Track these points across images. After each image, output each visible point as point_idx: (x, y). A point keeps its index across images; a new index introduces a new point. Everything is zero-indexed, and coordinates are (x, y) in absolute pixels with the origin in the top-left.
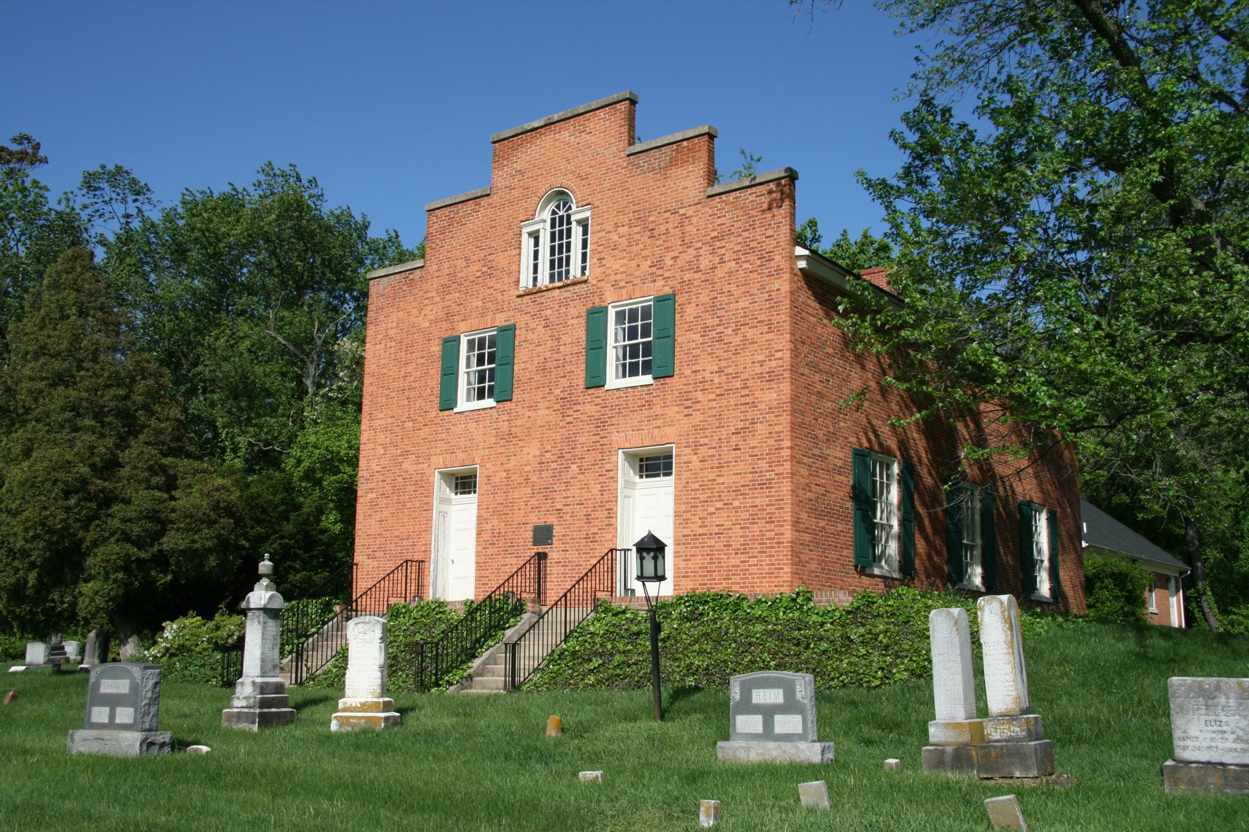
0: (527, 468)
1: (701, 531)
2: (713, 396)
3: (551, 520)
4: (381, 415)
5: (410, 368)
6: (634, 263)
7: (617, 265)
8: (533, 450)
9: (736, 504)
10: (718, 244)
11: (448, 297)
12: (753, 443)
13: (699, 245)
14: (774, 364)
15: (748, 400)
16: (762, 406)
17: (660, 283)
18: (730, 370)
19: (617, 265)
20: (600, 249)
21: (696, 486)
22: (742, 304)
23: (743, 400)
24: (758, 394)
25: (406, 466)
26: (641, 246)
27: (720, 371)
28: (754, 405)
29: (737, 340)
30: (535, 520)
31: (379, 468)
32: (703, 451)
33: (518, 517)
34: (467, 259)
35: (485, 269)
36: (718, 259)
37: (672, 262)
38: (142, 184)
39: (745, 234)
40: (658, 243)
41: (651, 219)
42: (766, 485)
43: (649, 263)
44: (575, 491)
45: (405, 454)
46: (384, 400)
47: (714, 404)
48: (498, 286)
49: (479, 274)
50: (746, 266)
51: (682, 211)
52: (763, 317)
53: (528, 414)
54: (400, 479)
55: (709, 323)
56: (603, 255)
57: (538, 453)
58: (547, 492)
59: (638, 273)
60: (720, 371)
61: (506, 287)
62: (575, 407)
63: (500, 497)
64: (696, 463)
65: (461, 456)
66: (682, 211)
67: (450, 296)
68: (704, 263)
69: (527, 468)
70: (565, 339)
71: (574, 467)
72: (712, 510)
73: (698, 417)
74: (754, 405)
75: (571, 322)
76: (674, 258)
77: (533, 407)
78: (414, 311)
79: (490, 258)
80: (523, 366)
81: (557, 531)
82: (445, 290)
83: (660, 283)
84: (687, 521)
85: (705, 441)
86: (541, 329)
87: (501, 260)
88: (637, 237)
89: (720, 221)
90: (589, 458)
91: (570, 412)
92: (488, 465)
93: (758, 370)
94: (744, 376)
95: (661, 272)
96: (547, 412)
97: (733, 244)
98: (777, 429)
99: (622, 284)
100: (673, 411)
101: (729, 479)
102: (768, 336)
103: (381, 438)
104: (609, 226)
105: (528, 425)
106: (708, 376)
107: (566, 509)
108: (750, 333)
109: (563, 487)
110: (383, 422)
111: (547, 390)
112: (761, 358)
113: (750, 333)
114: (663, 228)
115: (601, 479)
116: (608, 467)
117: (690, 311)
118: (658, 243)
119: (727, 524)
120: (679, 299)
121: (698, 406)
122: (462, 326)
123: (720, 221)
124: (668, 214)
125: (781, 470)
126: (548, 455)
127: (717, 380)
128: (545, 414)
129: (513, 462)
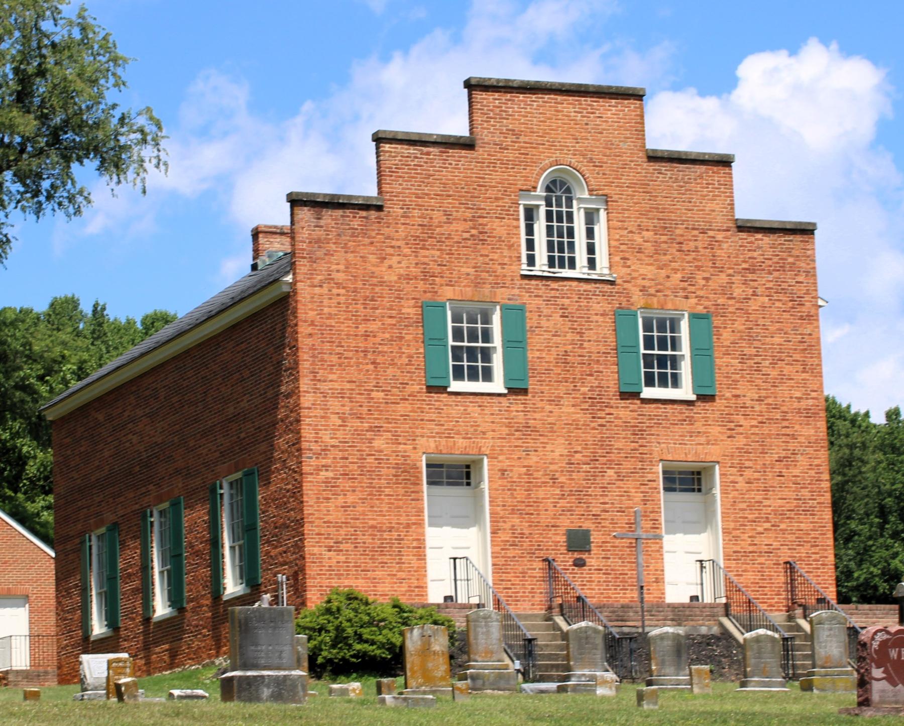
0: (552, 467)
1: (751, 549)
2: (754, 423)
3: (587, 525)
4: (331, 377)
5: (373, 326)
6: (663, 273)
7: (644, 270)
8: (558, 449)
9: (783, 526)
10: (750, 276)
11: (423, 252)
12: (796, 472)
13: (731, 271)
14: (811, 402)
15: (788, 431)
16: (802, 439)
17: (693, 301)
18: (770, 401)
19: (644, 270)
20: (623, 247)
21: (743, 506)
22: (777, 340)
23: (784, 431)
24: (797, 427)
25: (379, 443)
26: (669, 257)
27: (760, 400)
28: (794, 437)
29: (774, 373)
30: (567, 523)
31: (334, 442)
32: (748, 473)
33: (545, 519)
34: (447, 214)
35: (474, 232)
36: (750, 291)
37: (703, 282)
38: (878, 418)
39: (776, 274)
40: (689, 258)
41: (678, 232)
42: (810, 512)
43: (679, 276)
44: (613, 495)
45: (376, 430)
46: (334, 359)
47: (756, 430)
48: (496, 257)
49: (466, 235)
50: (778, 304)
51: (711, 233)
52: (797, 356)
53: (548, 408)
54: (370, 460)
55: (747, 351)
56: (627, 255)
57: (565, 452)
58: (580, 495)
59: (668, 284)
60: (760, 400)
61: (506, 260)
62: (608, 410)
63: (520, 494)
64: (741, 485)
65: (461, 442)
66: (711, 233)
67: (427, 253)
68: (738, 292)
69: (552, 467)
70: (588, 335)
71: (610, 472)
72: (760, 529)
73: (741, 441)
74: (794, 437)
75: (595, 318)
76: (707, 279)
77: (556, 401)
78: (372, 258)
79: (481, 221)
80: (537, 354)
81: (595, 538)
82: (419, 243)
83: (693, 301)
84: (736, 538)
85: (747, 464)
86: (557, 317)
87: (498, 228)
88: (664, 246)
89: (750, 254)
90: (628, 465)
91: (601, 414)
92: (501, 458)
93: (796, 405)
94: (784, 409)
95: (692, 289)
96: (572, 410)
97: (765, 280)
98: (816, 462)
99: (652, 291)
100: (715, 430)
101: (774, 502)
102: (804, 376)
103: (335, 405)
104: (632, 225)
105: (551, 420)
106: (749, 403)
107: (604, 515)
108: (787, 370)
109: (599, 492)
110: (336, 385)
111: (571, 387)
112: (798, 395)
113: (787, 370)
114: (692, 245)
115: (643, 488)
116: (650, 476)
117: (726, 336)
118: (689, 258)
119: (776, 544)
120: (717, 321)
121: (741, 430)
122: (448, 292)
123: (750, 254)
124: (696, 232)
125: (822, 499)
126: (578, 456)
127: (757, 408)
128: (568, 410)
129: (534, 459)
